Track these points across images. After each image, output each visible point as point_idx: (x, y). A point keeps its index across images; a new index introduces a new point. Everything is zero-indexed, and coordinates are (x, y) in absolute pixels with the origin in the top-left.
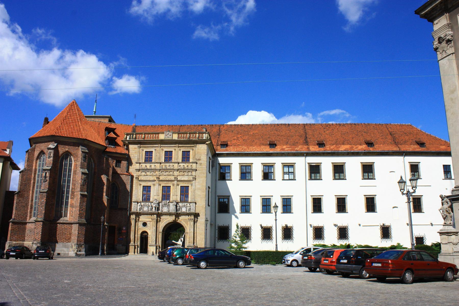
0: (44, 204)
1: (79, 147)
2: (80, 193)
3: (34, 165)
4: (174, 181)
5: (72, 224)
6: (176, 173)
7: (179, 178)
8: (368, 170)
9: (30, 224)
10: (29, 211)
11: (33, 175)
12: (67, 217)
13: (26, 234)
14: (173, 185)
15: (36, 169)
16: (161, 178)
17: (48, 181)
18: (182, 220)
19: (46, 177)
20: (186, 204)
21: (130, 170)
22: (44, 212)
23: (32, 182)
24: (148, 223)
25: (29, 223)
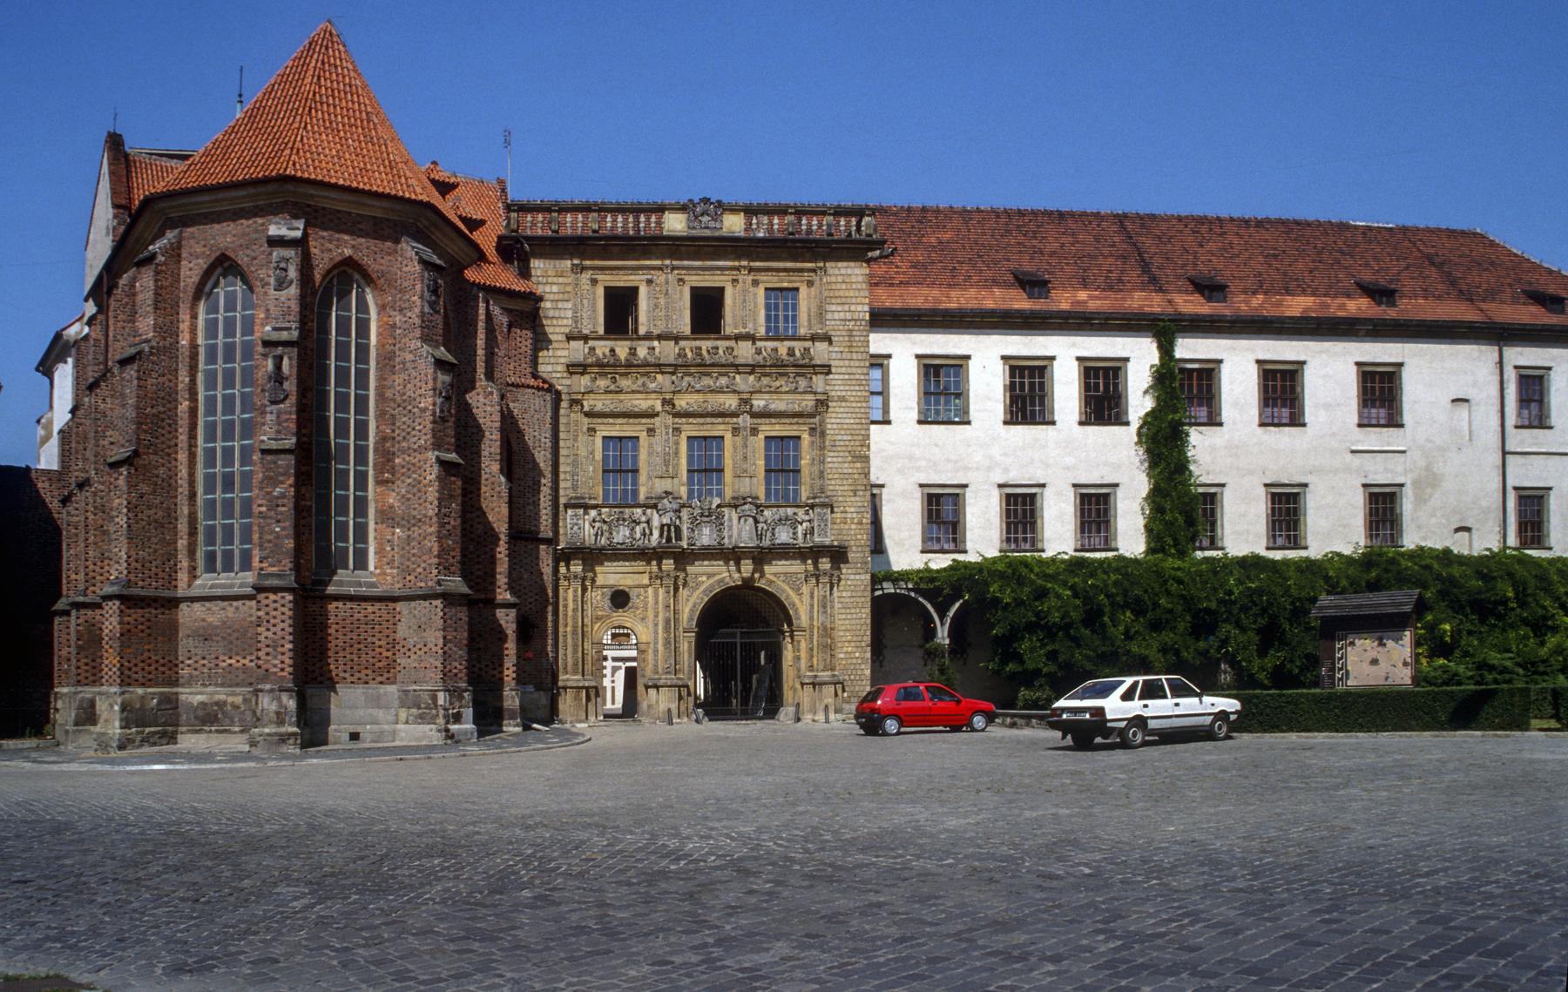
0: (287, 509)
1: (397, 241)
2: (432, 456)
3: (184, 326)
4: (735, 415)
5: (395, 599)
6: (744, 382)
7: (759, 403)
8: (1380, 394)
9: (197, 606)
10: (182, 543)
11: (184, 378)
12: (365, 568)
13: (181, 650)
14: (736, 431)
15: (194, 347)
16: (682, 402)
17: (293, 399)
18: (779, 577)
19: (278, 377)
20: (790, 511)
21: (541, 368)
22: (289, 544)
23: (184, 406)
24: (633, 593)
25: (193, 600)
